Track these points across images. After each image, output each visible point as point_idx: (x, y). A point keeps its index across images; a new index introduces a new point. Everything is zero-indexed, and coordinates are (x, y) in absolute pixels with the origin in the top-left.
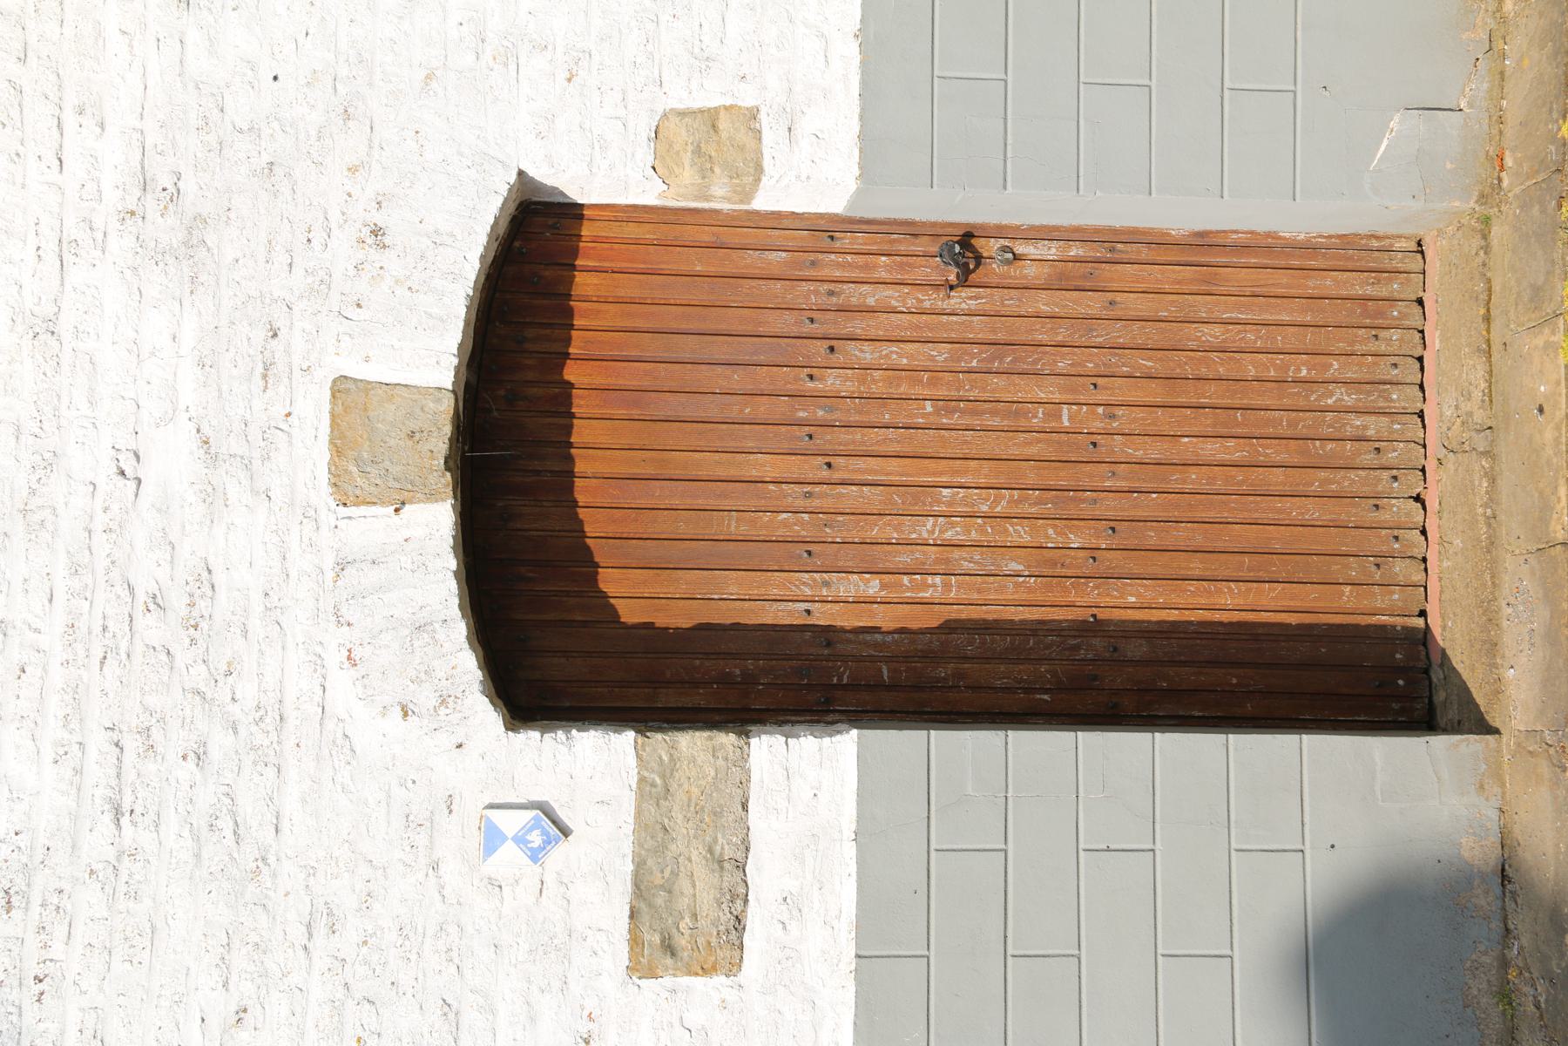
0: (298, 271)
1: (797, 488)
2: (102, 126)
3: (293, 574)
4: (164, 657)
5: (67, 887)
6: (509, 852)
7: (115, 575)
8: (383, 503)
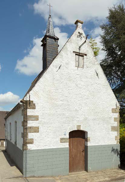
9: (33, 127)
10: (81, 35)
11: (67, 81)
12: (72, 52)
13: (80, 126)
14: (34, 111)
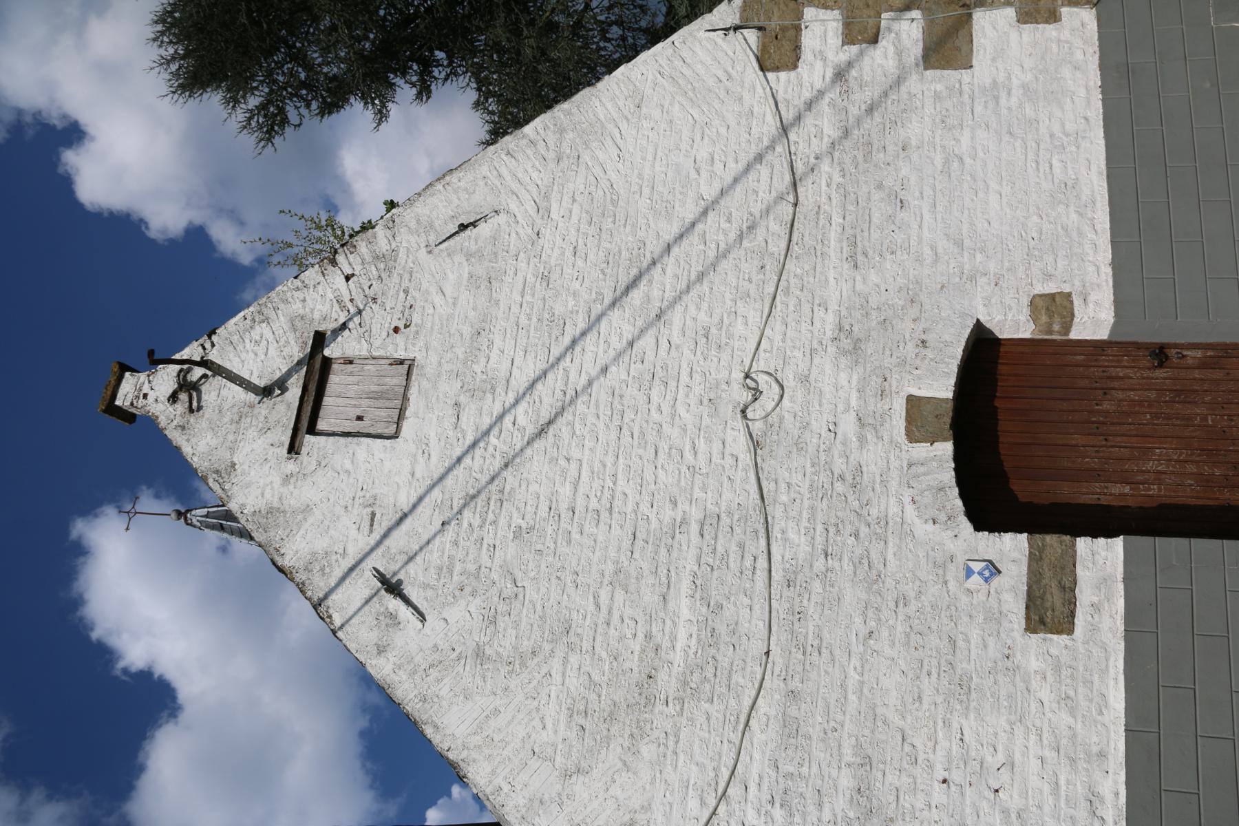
0: (894, 357)
1: (1092, 449)
2: (826, 310)
3: (892, 467)
4: (843, 498)
5: (809, 581)
6: (976, 578)
7: (827, 467)
8: (926, 442)
12: (291, 467)
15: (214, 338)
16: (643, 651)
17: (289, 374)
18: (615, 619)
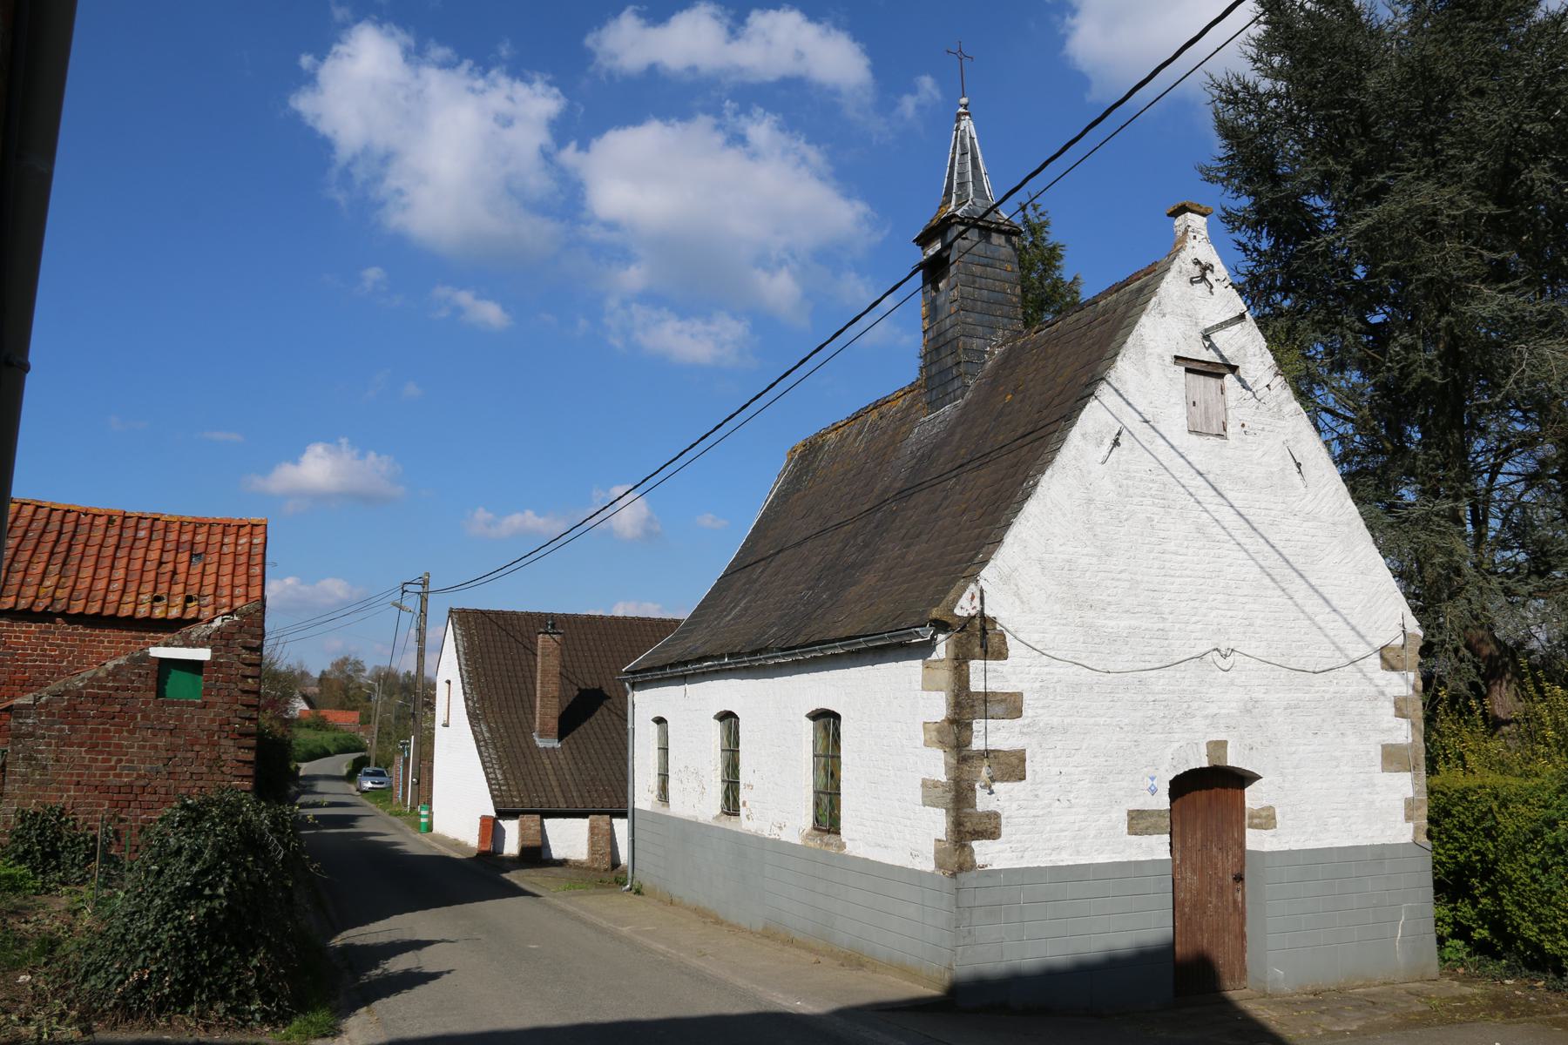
9: (999, 751)
10: (1209, 276)
11: (1155, 509)
12: (1169, 360)
13: (1222, 745)
14: (999, 669)
15: (1230, 287)
16: (1103, 601)
17: (1216, 350)
18: (1117, 583)
